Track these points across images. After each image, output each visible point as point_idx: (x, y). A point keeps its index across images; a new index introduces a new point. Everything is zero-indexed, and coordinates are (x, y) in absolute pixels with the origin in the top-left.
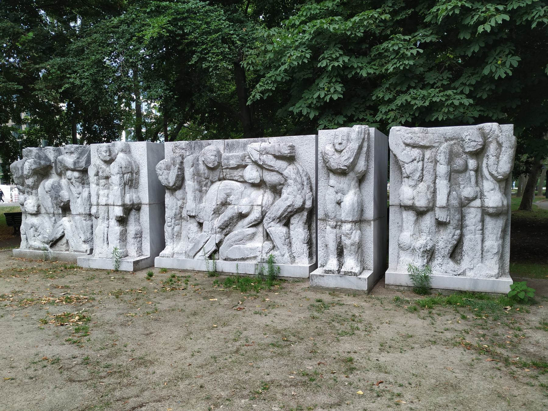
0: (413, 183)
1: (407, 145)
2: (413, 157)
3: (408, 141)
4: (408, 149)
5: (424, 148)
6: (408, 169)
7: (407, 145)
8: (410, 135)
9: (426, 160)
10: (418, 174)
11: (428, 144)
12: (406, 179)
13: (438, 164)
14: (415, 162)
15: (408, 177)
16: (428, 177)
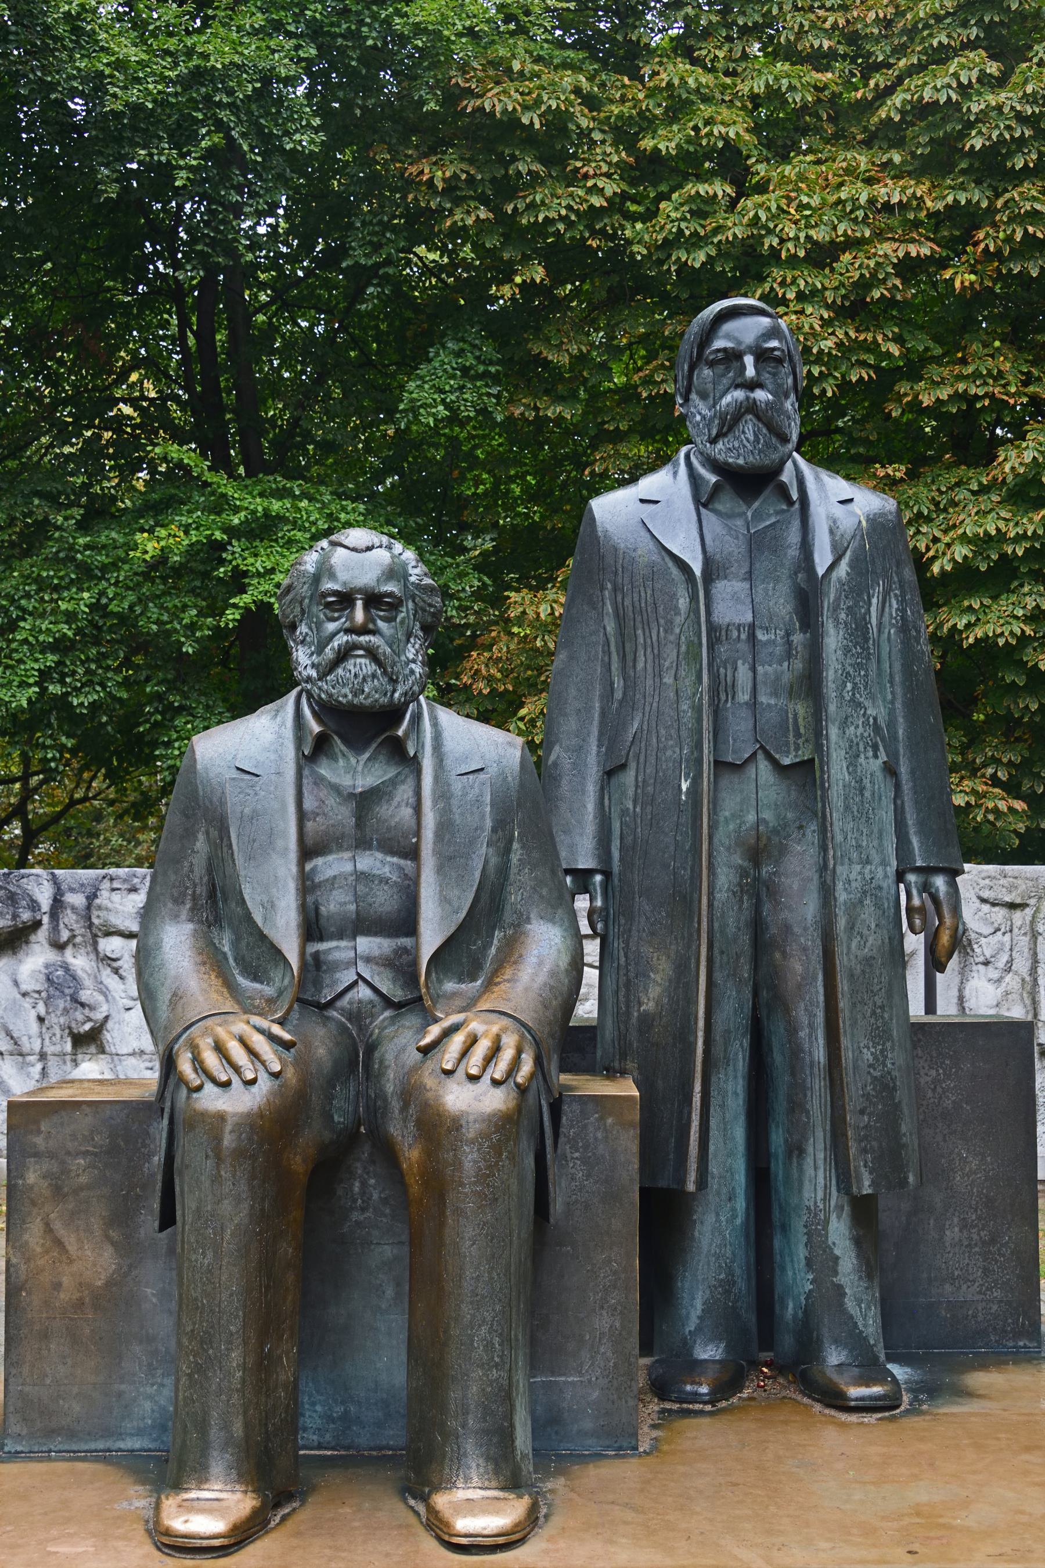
0: (995, 975)
1: (984, 901)
2: (996, 925)
3: (986, 894)
4: (986, 908)
5: (1012, 906)
6: (984, 947)
7: (984, 901)
8: (987, 881)
9: (1016, 930)
10: (1004, 958)
11: (1018, 901)
12: (981, 967)
13: (1040, 938)
14: (999, 933)
15: (986, 963)
16: (1022, 965)
